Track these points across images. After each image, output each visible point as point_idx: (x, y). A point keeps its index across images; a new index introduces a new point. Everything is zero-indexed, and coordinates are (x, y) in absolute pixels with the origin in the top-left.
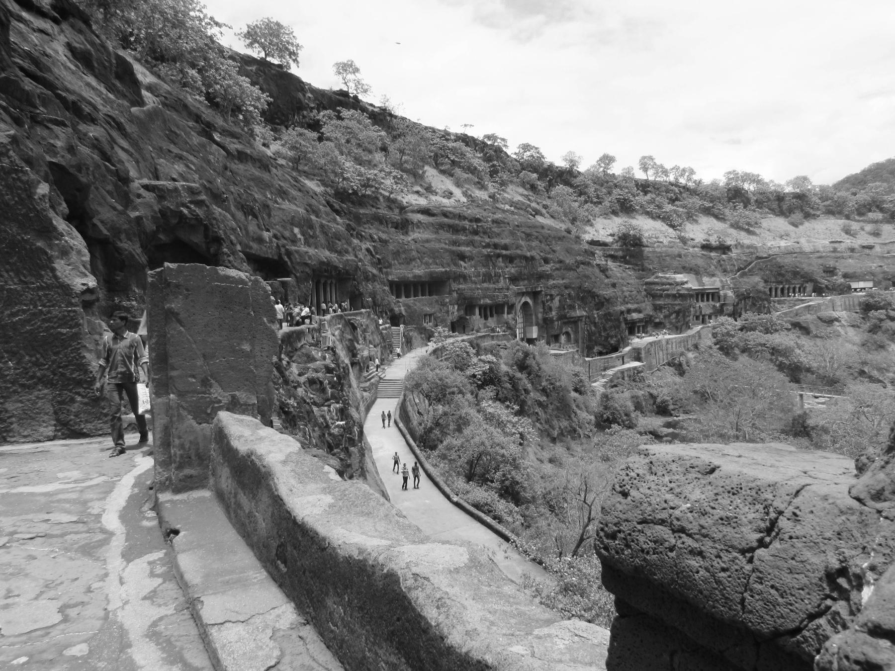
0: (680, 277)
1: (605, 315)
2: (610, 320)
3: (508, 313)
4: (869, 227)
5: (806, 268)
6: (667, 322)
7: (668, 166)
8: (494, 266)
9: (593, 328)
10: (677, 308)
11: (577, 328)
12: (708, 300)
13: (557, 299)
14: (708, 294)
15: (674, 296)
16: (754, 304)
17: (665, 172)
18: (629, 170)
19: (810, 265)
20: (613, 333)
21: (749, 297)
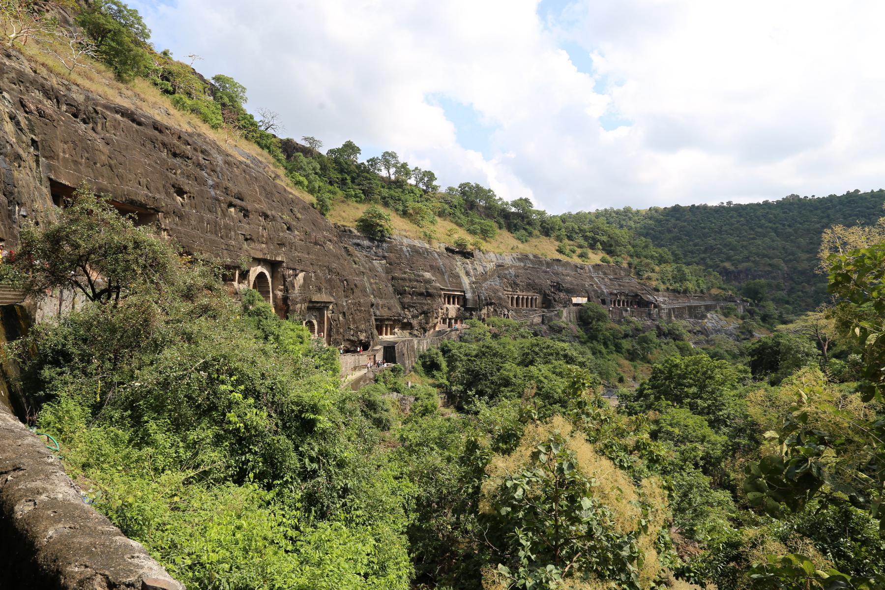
0: (428, 275)
1: (355, 304)
2: (360, 311)
3: (239, 283)
4: (579, 251)
5: (536, 281)
6: (415, 322)
7: (411, 167)
8: (224, 214)
9: (341, 318)
10: (426, 308)
11: (322, 316)
12: (454, 303)
13: (301, 276)
14: (454, 296)
15: (421, 294)
16: (495, 310)
17: (408, 174)
18: (373, 161)
19: (539, 277)
20: (363, 327)
21: (491, 304)
